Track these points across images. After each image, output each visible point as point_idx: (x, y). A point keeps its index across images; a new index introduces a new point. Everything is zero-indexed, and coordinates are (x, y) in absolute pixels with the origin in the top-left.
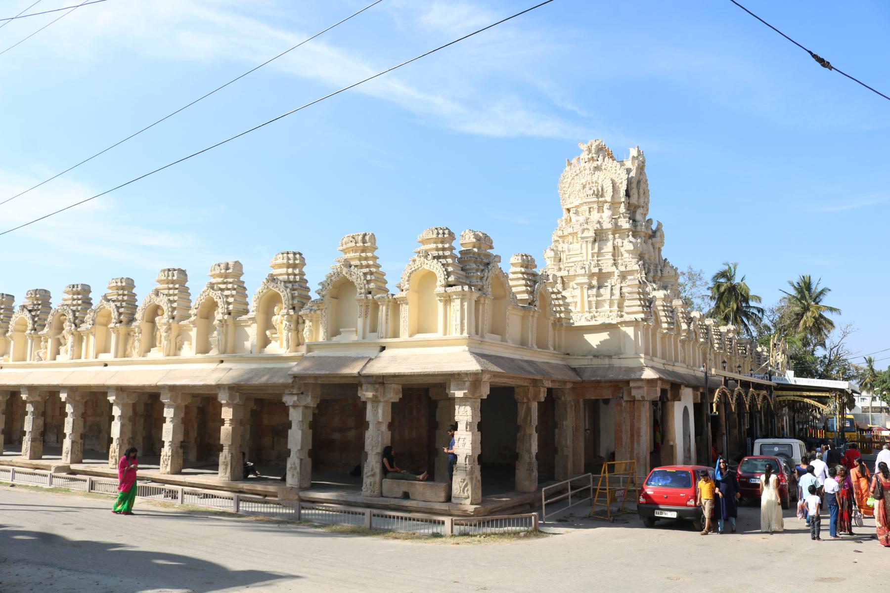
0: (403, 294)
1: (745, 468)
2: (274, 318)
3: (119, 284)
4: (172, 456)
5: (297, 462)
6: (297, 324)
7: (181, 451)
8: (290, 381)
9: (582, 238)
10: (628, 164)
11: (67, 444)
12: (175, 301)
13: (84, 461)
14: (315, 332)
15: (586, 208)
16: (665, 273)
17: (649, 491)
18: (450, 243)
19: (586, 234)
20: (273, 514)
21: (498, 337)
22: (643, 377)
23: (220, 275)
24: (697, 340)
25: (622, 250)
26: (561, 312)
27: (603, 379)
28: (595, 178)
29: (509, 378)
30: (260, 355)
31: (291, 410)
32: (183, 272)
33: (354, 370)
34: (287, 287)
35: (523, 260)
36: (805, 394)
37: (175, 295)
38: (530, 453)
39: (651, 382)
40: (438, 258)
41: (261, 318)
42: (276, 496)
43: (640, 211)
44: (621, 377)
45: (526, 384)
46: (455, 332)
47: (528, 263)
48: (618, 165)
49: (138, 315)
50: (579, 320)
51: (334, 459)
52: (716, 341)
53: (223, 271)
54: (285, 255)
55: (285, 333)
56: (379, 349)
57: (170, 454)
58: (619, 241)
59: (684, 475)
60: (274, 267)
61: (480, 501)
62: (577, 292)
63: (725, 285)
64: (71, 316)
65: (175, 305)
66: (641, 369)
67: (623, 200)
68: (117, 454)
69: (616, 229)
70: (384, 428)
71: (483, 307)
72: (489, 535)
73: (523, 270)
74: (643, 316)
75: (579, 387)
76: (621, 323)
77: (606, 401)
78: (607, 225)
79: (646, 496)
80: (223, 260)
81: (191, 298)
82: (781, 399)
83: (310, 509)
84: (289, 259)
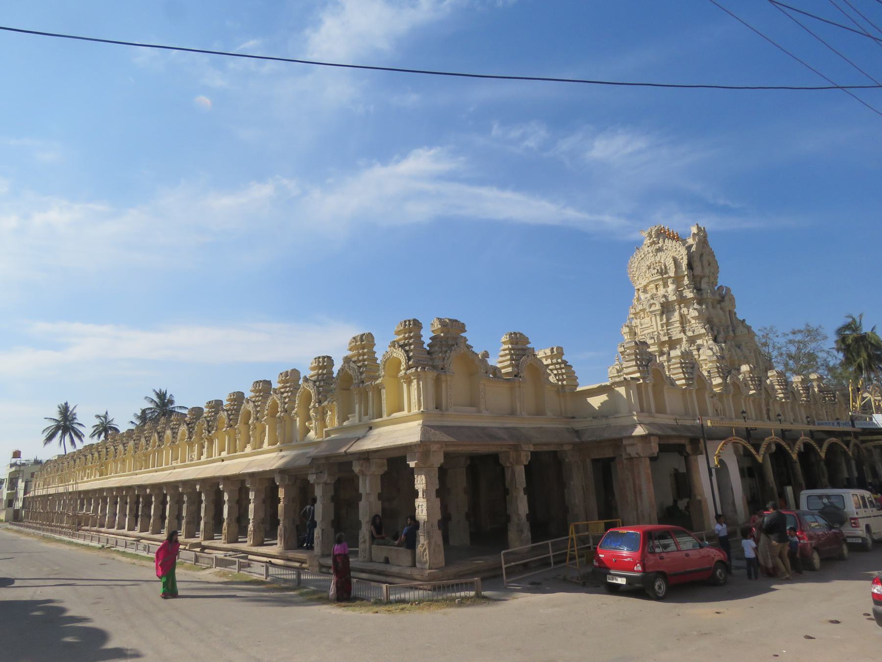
8: (309, 461)
9: (651, 312)
14: (332, 420)
15: (652, 285)
16: (738, 332)
19: (653, 308)
21: (474, 409)
25: (689, 317)
26: (563, 380)
28: (658, 259)
33: (343, 450)
35: (511, 338)
38: (518, 515)
39: (642, 437)
42: (306, 563)
44: (615, 436)
45: (504, 449)
46: (415, 410)
52: (780, 391)
58: (684, 310)
61: (444, 564)
63: (851, 337)
65: (258, 409)
66: (634, 427)
69: (682, 300)
70: (373, 498)
75: (581, 447)
78: (672, 298)
80: (285, 371)
84: (319, 362)
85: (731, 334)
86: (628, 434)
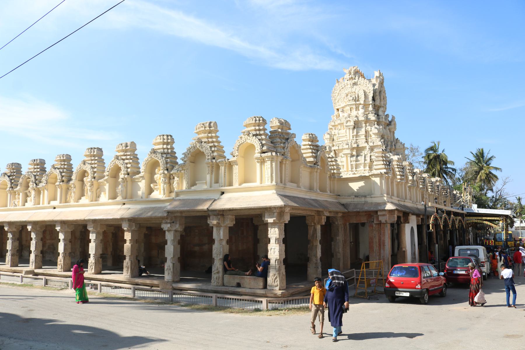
0: (235, 159)
1: (450, 264)
2: (156, 176)
3: (62, 158)
4: (95, 263)
5: (171, 265)
6: (170, 179)
7: (101, 260)
8: (165, 215)
10: (374, 81)
11: (32, 257)
12: (95, 168)
13: (43, 267)
14: (181, 184)
15: (348, 108)
16: (397, 147)
17: (392, 280)
18: (264, 126)
19: (348, 124)
20: (156, 298)
21: (295, 185)
22: (386, 208)
23: (122, 151)
24: (418, 186)
25: (371, 133)
26: (334, 169)
27: (361, 210)
28: (353, 90)
29: (302, 210)
30: (147, 199)
31: (167, 233)
32: (100, 150)
33: (204, 207)
34: (163, 157)
35: (310, 137)
36: (484, 218)
37: (95, 164)
38: (316, 257)
40: (256, 135)
41: (147, 176)
42: (159, 287)
43: (381, 109)
44: (372, 209)
45: (313, 214)
46: (267, 182)
47: (313, 139)
48: (368, 82)
49: (73, 177)
50: (344, 175)
51: (194, 264)
52: (429, 187)
53: (124, 148)
54: (162, 137)
55: (162, 185)
56: (220, 193)
57: (94, 262)
58: (369, 128)
59: (413, 269)
60: (155, 144)
62: (344, 159)
64: (33, 179)
65: (95, 170)
66: (385, 204)
67: (371, 103)
68: (62, 262)
69: (367, 120)
70: (224, 243)
71: (285, 166)
72: (291, 309)
73: (310, 143)
74: (385, 171)
75: (346, 215)
76: (372, 175)
77: (363, 224)
78: (362, 118)
79: (390, 283)
80: (124, 142)
81: (105, 165)
82: (469, 222)
83: (180, 294)
84: (164, 139)
85: (394, 147)
86: (383, 209)
